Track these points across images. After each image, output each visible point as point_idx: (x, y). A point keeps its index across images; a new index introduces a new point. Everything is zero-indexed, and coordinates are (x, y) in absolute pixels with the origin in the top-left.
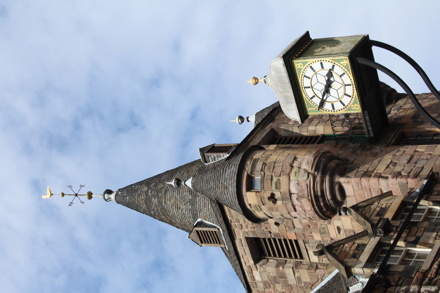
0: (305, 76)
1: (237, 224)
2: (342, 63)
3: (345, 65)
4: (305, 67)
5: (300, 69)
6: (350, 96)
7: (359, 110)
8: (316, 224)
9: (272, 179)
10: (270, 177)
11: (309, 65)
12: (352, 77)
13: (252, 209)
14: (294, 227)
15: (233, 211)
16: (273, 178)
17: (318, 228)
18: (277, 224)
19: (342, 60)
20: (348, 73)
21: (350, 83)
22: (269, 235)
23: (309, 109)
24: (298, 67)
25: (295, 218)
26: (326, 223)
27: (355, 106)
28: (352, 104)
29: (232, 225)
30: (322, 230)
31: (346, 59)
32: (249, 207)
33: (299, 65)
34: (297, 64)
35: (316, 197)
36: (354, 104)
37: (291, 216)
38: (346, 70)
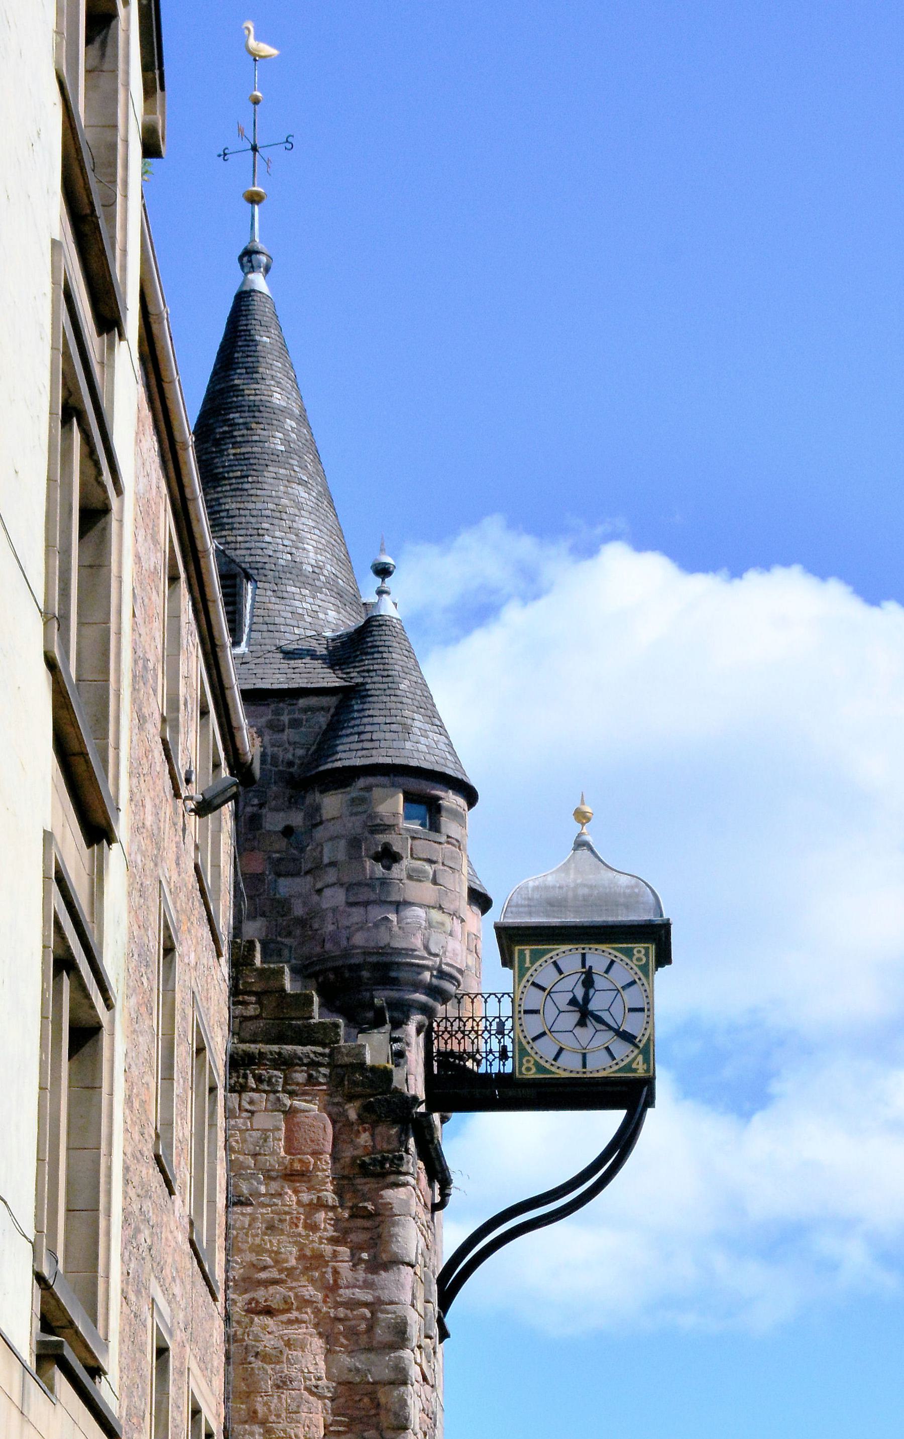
0: (612, 962)
1: (285, 718)
2: (640, 1058)
3: (634, 1066)
4: (634, 967)
5: (629, 953)
6: (555, 1059)
7: (520, 1072)
8: (289, 934)
9: (431, 862)
10: (435, 859)
11: (640, 979)
12: (602, 1074)
13: (354, 791)
14: (279, 875)
15: (323, 720)
16: (433, 866)
17: (279, 939)
18: (288, 831)
19: (647, 1060)
20: (616, 1068)
21: (589, 1067)
22: (256, 801)
23: (527, 949)
24: (635, 952)
25: (319, 891)
26: (294, 961)
27: (531, 1065)
28: (536, 1061)
29: (281, 705)
30: (272, 946)
31: (647, 1071)
32: (362, 782)
33: (642, 955)
34: (643, 951)
35: (387, 967)
36: (537, 1064)
37: (328, 886)
38: (622, 1064)
